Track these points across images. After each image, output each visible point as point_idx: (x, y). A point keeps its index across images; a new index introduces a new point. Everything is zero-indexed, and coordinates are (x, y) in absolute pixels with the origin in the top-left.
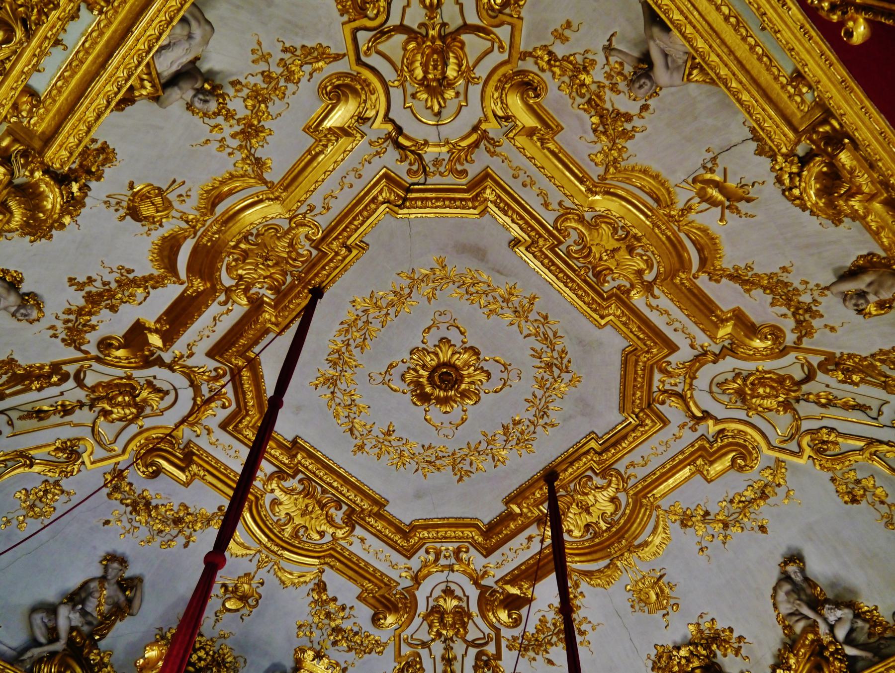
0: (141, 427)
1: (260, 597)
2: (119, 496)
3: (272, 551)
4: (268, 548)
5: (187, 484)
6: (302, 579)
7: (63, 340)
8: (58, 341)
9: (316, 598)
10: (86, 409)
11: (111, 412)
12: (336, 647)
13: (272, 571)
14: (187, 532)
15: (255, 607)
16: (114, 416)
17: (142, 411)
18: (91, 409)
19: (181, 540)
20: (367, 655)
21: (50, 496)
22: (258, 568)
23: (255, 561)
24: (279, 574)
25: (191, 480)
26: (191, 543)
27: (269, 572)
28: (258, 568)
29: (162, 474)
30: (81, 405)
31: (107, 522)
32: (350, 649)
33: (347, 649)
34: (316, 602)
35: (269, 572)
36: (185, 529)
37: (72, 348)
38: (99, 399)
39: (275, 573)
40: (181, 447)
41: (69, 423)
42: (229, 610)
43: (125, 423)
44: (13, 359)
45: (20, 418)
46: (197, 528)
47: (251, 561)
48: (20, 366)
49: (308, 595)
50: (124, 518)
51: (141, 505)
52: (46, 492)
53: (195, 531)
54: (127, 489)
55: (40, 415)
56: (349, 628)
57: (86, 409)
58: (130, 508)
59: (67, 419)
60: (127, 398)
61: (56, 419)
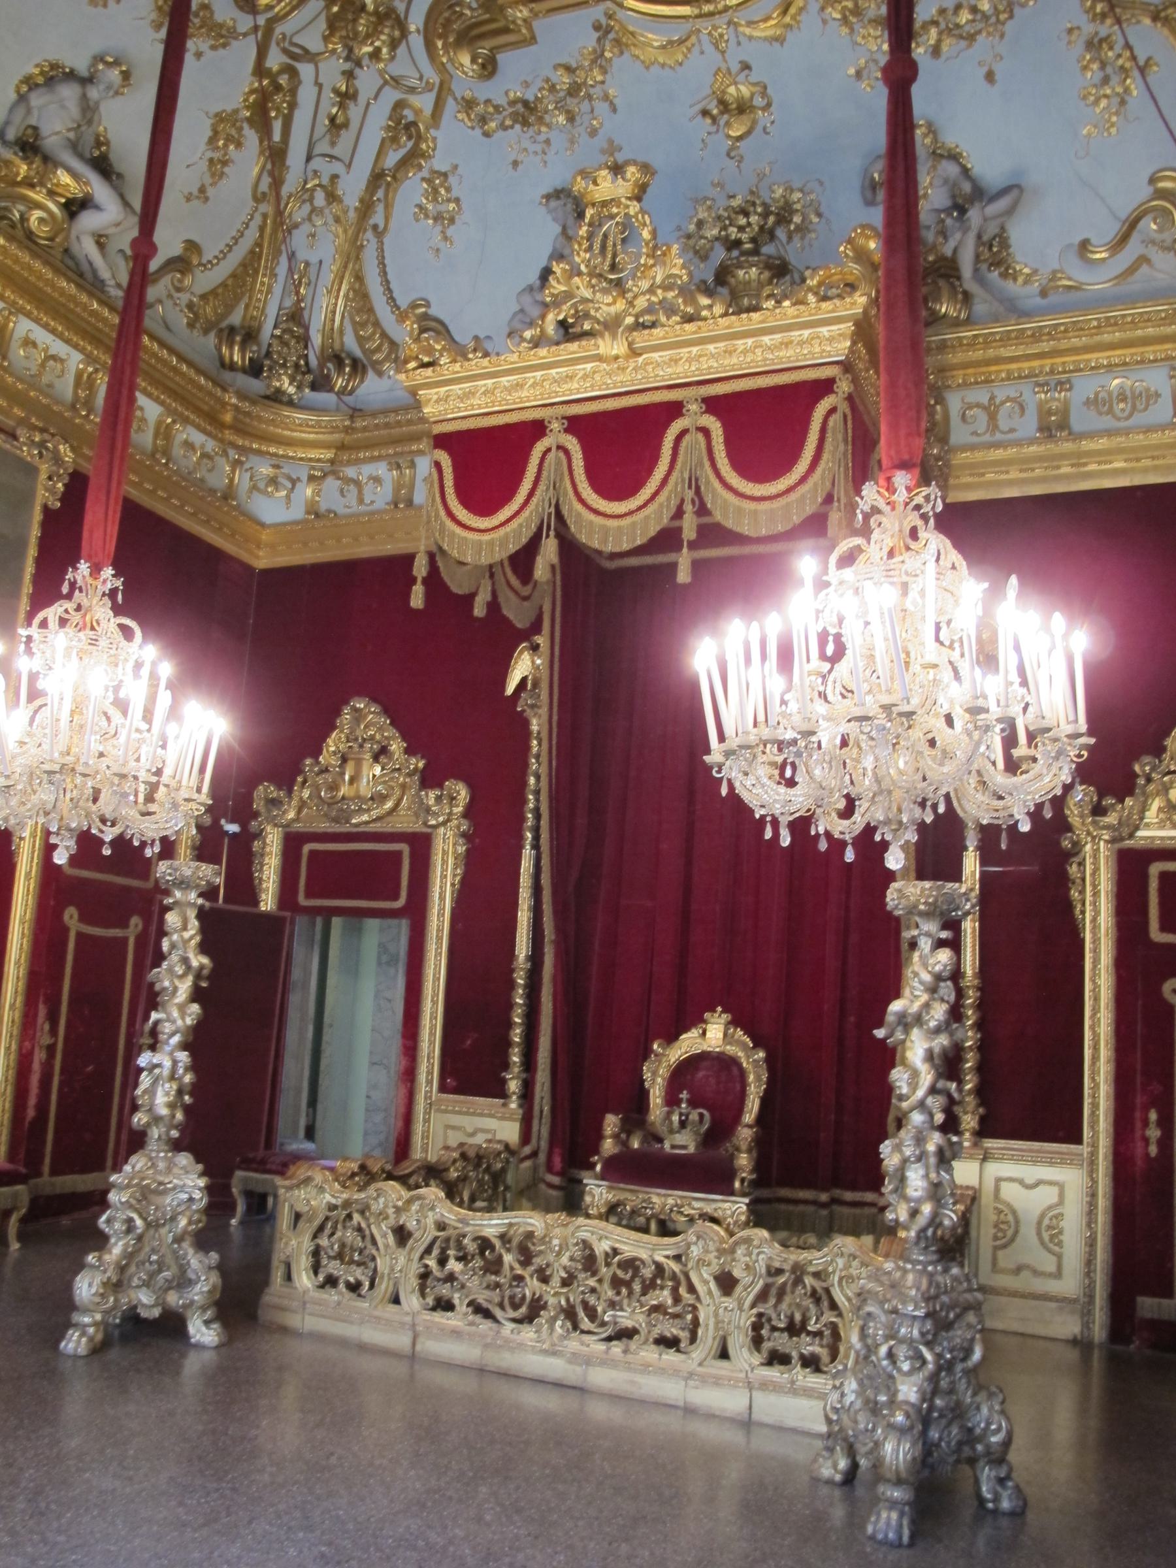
0: (418, 31)
1: (765, 87)
2: (493, 125)
3: (711, 14)
4: (700, 16)
5: (532, 40)
6: (792, 10)
7: (213, 48)
8: (209, 54)
9: (838, 16)
10: (357, 71)
11: (378, 51)
12: (943, 57)
13: (741, 38)
14: (597, 92)
15: (769, 105)
16: (385, 50)
17: (398, 17)
18: (361, 67)
19: (602, 108)
20: (1010, 24)
21: (443, 191)
22: (723, 52)
23: (709, 48)
24: (756, 34)
25: (530, 29)
26: (616, 101)
27: (739, 43)
28: (723, 52)
29: (498, 57)
30: (349, 75)
31: (515, 164)
32: (971, 38)
33: (963, 43)
34: (845, 20)
35: (739, 43)
36: (592, 91)
37: (234, 43)
38: (351, 50)
39: (750, 38)
40: (474, 5)
41: (368, 104)
42: (739, 138)
43: (403, 46)
44: (217, 115)
45: (333, 144)
46: (599, 78)
47: (702, 53)
48: (236, 111)
49: (824, 22)
50: (526, 144)
51: (527, 113)
52: (435, 191)
53: (603, 82)
54: (491, 109)
55: (336, 126)
56: (934, 11)
57: (357, 71)
58: (518, 127)
59: (362, 99)
60: (362, 21)
61: (354, 112)
